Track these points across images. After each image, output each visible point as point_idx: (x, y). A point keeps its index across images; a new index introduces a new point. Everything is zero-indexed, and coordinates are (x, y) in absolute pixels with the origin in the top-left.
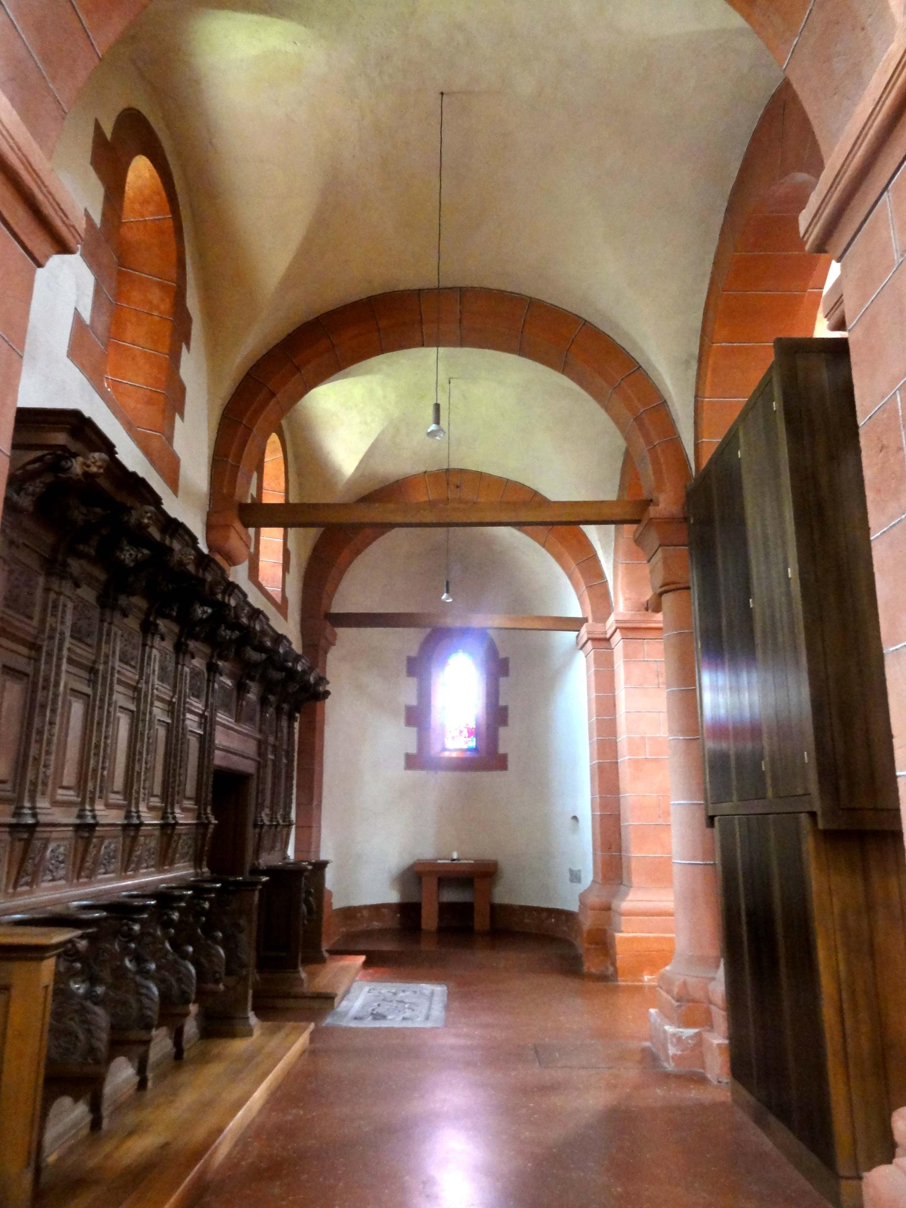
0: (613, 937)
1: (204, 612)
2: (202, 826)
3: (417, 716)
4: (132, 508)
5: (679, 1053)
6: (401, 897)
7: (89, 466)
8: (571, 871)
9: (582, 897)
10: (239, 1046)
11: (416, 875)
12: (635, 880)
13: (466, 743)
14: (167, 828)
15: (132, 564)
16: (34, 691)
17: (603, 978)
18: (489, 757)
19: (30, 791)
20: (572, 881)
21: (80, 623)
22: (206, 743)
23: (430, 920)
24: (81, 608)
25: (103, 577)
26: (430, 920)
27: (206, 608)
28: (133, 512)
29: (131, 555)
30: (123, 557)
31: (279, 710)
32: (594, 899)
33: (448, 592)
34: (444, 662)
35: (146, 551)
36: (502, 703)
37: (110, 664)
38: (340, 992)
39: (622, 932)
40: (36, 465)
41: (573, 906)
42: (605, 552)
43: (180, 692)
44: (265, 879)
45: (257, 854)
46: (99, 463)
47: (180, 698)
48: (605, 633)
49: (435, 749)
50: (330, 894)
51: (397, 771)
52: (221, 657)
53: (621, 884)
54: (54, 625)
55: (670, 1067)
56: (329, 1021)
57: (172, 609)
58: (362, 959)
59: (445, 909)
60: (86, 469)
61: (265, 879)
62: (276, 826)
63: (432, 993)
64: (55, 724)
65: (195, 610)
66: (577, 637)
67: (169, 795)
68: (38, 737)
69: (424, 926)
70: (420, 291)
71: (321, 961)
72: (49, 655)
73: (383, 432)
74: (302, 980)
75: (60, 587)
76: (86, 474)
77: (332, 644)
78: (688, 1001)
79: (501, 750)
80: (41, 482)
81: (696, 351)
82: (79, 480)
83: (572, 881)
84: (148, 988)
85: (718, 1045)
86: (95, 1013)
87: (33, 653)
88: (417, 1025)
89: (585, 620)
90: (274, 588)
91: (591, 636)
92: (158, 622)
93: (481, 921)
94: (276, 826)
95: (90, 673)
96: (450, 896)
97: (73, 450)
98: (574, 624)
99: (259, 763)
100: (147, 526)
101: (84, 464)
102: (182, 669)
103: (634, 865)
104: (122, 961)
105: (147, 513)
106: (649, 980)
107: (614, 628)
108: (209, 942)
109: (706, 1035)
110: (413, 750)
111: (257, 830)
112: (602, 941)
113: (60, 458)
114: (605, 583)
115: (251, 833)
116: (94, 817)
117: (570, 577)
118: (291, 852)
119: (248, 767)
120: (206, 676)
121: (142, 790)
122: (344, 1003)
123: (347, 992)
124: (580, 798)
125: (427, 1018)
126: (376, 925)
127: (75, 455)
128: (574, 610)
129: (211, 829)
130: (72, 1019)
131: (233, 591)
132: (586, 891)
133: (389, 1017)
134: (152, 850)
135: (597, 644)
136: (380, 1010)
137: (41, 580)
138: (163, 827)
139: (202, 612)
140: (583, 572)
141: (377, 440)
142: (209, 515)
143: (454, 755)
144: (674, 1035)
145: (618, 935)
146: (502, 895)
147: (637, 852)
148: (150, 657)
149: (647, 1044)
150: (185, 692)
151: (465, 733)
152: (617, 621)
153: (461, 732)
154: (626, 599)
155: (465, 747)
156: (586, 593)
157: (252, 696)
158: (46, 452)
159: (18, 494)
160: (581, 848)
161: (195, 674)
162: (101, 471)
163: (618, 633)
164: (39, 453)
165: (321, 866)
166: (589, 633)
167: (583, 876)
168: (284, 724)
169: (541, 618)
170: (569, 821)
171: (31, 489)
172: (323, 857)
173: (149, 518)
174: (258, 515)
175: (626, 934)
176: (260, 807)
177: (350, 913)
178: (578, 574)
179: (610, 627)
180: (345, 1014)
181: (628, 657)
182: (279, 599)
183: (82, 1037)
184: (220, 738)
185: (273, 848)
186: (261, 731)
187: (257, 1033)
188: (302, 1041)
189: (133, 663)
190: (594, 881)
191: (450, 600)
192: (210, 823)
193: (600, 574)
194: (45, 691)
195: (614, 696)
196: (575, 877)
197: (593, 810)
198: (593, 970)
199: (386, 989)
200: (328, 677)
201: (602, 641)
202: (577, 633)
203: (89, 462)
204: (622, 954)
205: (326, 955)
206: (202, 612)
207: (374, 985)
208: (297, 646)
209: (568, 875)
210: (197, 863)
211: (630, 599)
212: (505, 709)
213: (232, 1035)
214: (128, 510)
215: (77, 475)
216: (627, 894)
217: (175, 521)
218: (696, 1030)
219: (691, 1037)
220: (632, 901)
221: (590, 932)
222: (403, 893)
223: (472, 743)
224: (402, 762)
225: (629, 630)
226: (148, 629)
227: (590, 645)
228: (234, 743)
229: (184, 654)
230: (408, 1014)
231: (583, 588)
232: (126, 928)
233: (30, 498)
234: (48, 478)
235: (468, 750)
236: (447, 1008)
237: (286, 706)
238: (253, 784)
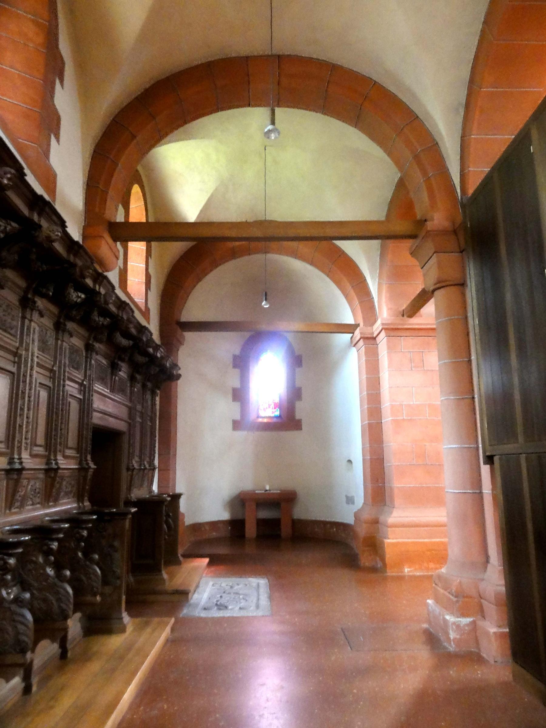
0: (383, 543)
1: (78, 297)
2: (82, 469)
3: (239, 395)
5: (458, 637)
8: (347, 497)
9: (357, 515)
10: (115, 642)
11: (241, 501)
14: (51, 472)
17: (374, 570)
18: (289, 420)
22: (85, 407)
23: (251, 530)
26: (251, 530)
31: (144, 386)
32: (366, 516)
33: (266, 300)
34: (257, 359)
35: (14, 225)
38: (192, 589)
39: (389, 539)
41: (350, 520)
42: (372, 278)
43: (60, 362)
44: (134, 510)
45: (129, 489)
47: (60, 367)
48: (373, 333)
49: (252, 416)
50: (183, 515)
52: (96, 339)
53: (385, 505)
55: (452, 648)
56: (185, 612)
57: (48, 290)
58: (207, 560)
59: (261, 523)
61: (134, 510)
63: (258, 585)
65: (69, 293)
66: (352, 338)
67: (52, 444)
69: (247, 535)
71: (179, 563)
73: (216, 189)
74: (164, 580)
77: (181, 343)
78: (464, 597)
84: (23, 616)
85: (494, 633)
88: (250, 614)
89: (356, 326)
91: (362, 336)
92: (36, 299)
93: (286, 530)
96: (264, 514)
98: (349, 329)
99: (130, 424)
102: (62, 345)
103: (396, 491)
106: (408, 572)
107: (381, 328)
108: (88, 563)
109: (481, 623)
110: (238, 417)
111: (130, 473)
112: (374, 545)
115: (125, 475)
117: (346, 296)
118: (155, 488)
119: (121, 426)
121: (24, 441)
122: (196, 596)
123: (197, 586)
125: (258, 607)
131: (102, 282)
132: (359, 510)
133: (230, 607)
134: (37, 490)
136: (223, 601)
138: (47, 471)
139: (76, 296)
141: (212, 195)
143: (265, 420)
144: (454, 623)
145: (387, 541)
147: (398, 483)
148: (29, 329)
149: (425, 626)
150: (65, 363)
151: (273, 406)
152: (383, 324)
154: (388, 309)
155: (273, 415)
156: (358, 306)
157: (123, 374)
160: (354, 481)
161: (73, 350)
163: (383, 334)
165: (176, 497)
166: (361, 333)
167: (356, 499)
168: (148, 396)
169: (329, 325)
170: (345, 462)
172: (178, 491)
173: (9, 179)
174: (125, 233)
175: (392, 540)
176: (130, 457)
177: (196, 527)
178: (352, 293)
179: (376, 330)
180: (197, 605)
181: (390, 348)
182: (143, 308)
184: (97, 403)
185: (141, 485)
186: (131, 401)
187: (129, 629)
188: (166, 633)
189: (12, 332)
191: (267, 306)
192: (90, 467)
195: (379, 378)
196: (350, 500)
197: (364, 455)
198: (367, 564)
199: (225, 582)
200: (180, 365)
202: (351, 335)
204: (389, 554)
205: (181, 559)
206: (76, 296)
207: (216, 580)
209: (344, 499)
210: (80, 498)
211: (391, 309)
213: (108, 631)
216: (392, 513)
218: (472, 619)
219: (467, 625)
220: (395, 517)
222: (232, 514)
223: (277, 413)
224: (230, 425)
225: (391, 330)
226: (26, 304)
227: (361, 343)
230: (243, 604)
231: (356, 302)
235: (276, 417)
236: (271, 598)
237: (149, 385)
238: (126, 438)
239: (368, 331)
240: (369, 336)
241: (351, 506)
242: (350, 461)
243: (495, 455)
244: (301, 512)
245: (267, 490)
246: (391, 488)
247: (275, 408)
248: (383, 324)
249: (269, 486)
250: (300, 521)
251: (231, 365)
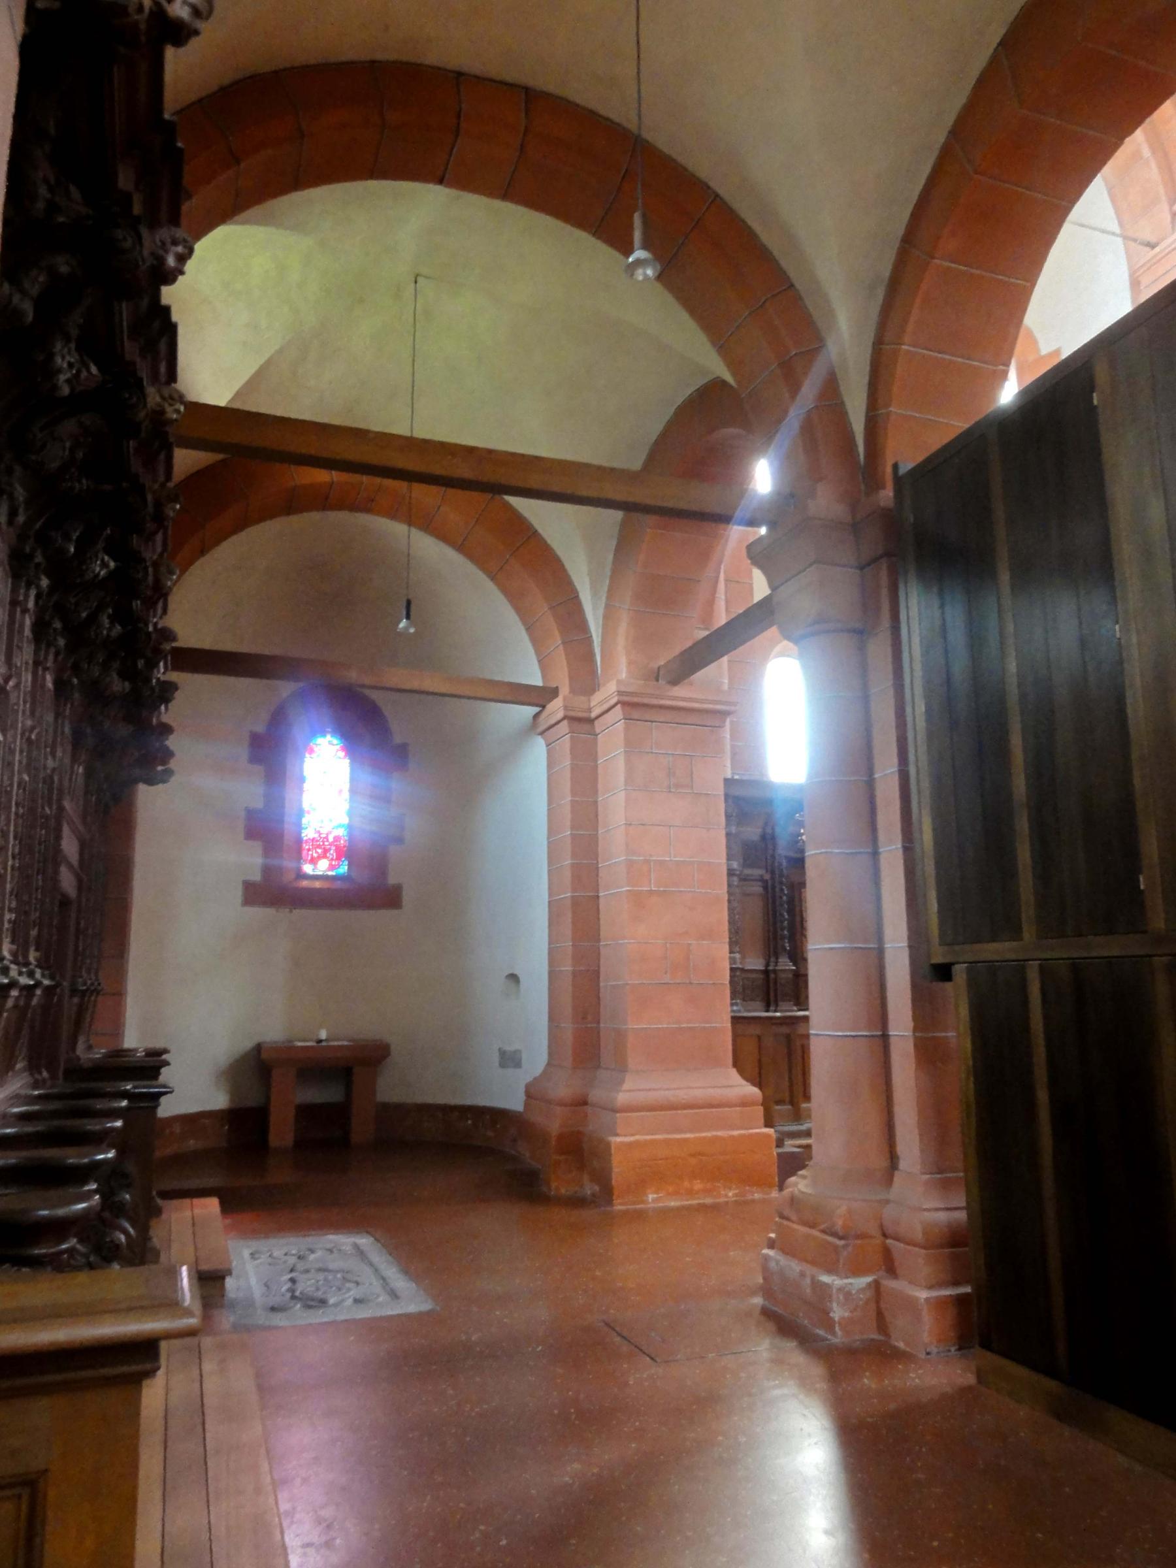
0: (608, 1145)
5: (846, 1314)
6: (232, 1100)
8: (502, 1053)
11: (258, 1067)
12: (632, 1062)
13: (332, 868)
17: (578, 1202)
20: (503, 1065)
26: (282, 1132)
33: (408, 617)
39: (617, 1135)
41: (515, 1102)
42: (595, 594)
48: (590, 710)
51: (230, 909)
53: (598, 1067)
55: (838, 1338)
57: (67, 537)
59: (306, 1112)
66: (536, 716)
69: (274, 1140)
70: (459, 75)
73: (280, 351)
78: (858, 1237)
81: (887, 273)
83: (503, 1065)
85: (927, 1299)
93: (361, 1129)
106: (654, 1200)
109: (890, 1284)
111: (76, 1000)
112: (581, 1150)
114: (589, 639)
126: (192, 1144)
133: (332, 1301)
141: (268, 363)
143: (317, 885)
144: (840, 1289)
147: (635, 1022)
152: (620, 693)
153: (326, 851)
154: (629, 663)
155: (330, 873)
166: (566, 708)
167: (524, 1057)
175: (626, 1139)
179: (601, 703)
181: (632, 746)
193: (583, 626)
198: (563, 1191)
202: (537, 709)
209: (496, 1058)
216: (622, 1082)
218: (869, 1279)
219: (862, 1290)
220: (629, 1091)
221: (561, 1137)
222: (235, 1092)
223: (343, 869)
224: (238, 894)
225: (631, 705)
240: (580, 715)
241: (510, 1071)
242: (514, 978)
243: (953, 964)
244: (392, 1087)
245: (320, 1041)
247: (339, 858)
248: (620, 693)
249: (324, 1030)
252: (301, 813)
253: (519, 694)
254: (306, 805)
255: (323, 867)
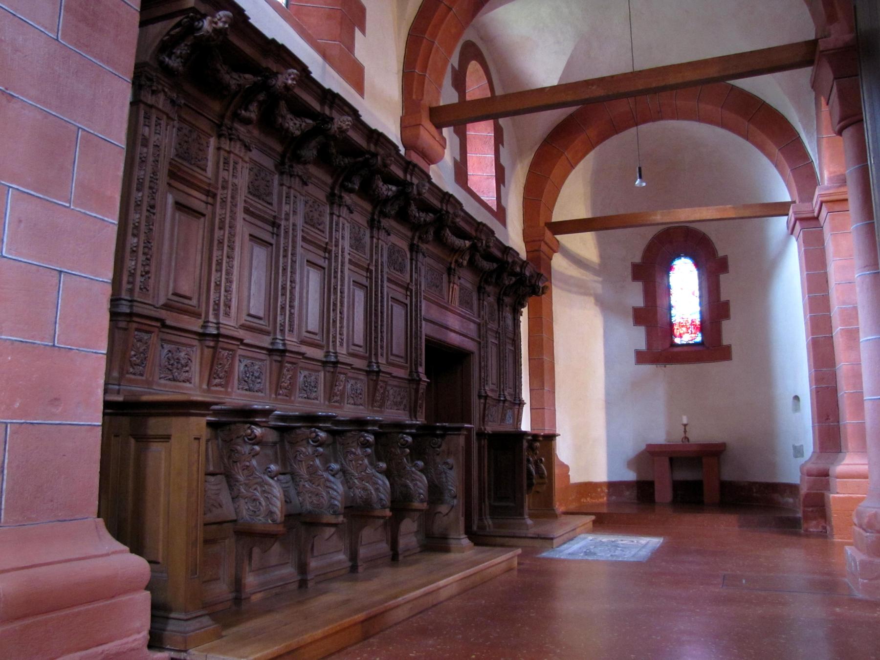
1: (388, 190)
4: (277, 73)
7: (216, 23)
8: (795, 447)
15: (298, 133)
16: (212, 231)
18: (712, 346)
19: (214, 310)
21: (256, 183)
23: (664, 493)
24: (258, 170)
25: (279, 148)
27: (390, 187)
28: (280, 76)
29: (295, 124)
30: (287, 125)
31: (500, 302)
32: (813, 467)
33: (640, 177)
36: (723, 298)
37: (291, 221)
40: (177, 30)
42: (808, 133)
43: (377, 261)
46: (223, 19)
47: (376, 266)
48: (813, 211)
50: (566, 468)
54: (226, 178)
60: (214, 25)
62: (504, 401)
64: (233, 258)
65: (377, 186)
68: (218, 268)
69: (657, 498)
72: (224, 201)
75: (230, 146)
76: (215, 30)
79: (725, 342)
80: (186, 45)
82: (210, 36)
83: (796, 457)
86: (270, 485)
87: (210, 200)
90: (490, 198)
91: (798, 216)
92: (343, 194)
94: (504, 401)
95: (273, 227)
96: (685, 475)
97: (203, 12)
100: (347, 130)
101: (212, 22)
102: (377, 244)
104: (314, 461)
105: (290, 75)
108: (413, 469)
110: (642, 346)
111: (482, 401)
113: (193, 20)
116: (284, 345)
119: (470, 345)
120: (408, 256)
121: (338, 336)
124: (795, 373)
127: (204, 16)
128: (784, 195)
129: (423, 386)
130: (255, 489)
131: (413, 170)
134: (359, 392)
135: (805, 224)
137: (213, 141)
140: (789, 159)
141: (572, 57)
142: (402, 119)
146: (728, 474)
148: (337, 224)
150: (382, 262)
156: (791, 176)
158: (182, 17)
159: (170, 58)
161: (393, 250)
162: (227, 26)
164: (178, 19)
165: (550, 438)
166: (795, 213)
169: (746, 207)
170: (790, 401)
171: (179, 52)
173: (293, 79)
175: (837, 495)
176: (483, 381)
178: (781, 158)
182: (495, 208)
183: (264, 503)
190: (814, 452)
191: (644, 184)
192: (420, 380)
193: (805, 156)
194: (222, 232)
195: (826, 273)
196: (798, 451)
201: (809, 223)
203: (216, 20)
208: (523, 255)
209: (792, 451)
212: (727, 304)
214: (275, 75)
215: (208, 32)
217: (330, 91)
221: (807, 495)
222: (638, 472)
223: (699, 338)
226: (333, 199)
228: (457, 327)
229: (379, 229)
231: (788, 171)
232: (314, 434)
233: (179, 60)
234: (189, 41)
238: (475, 359)
239: (805, 209)
242: (796, 398)
246: (845, 425)
250: (731, 484)
251: (630, 277)
252: (670, 307)
253: (781, 209)
254: (673, 303)
255: (686, 339)
